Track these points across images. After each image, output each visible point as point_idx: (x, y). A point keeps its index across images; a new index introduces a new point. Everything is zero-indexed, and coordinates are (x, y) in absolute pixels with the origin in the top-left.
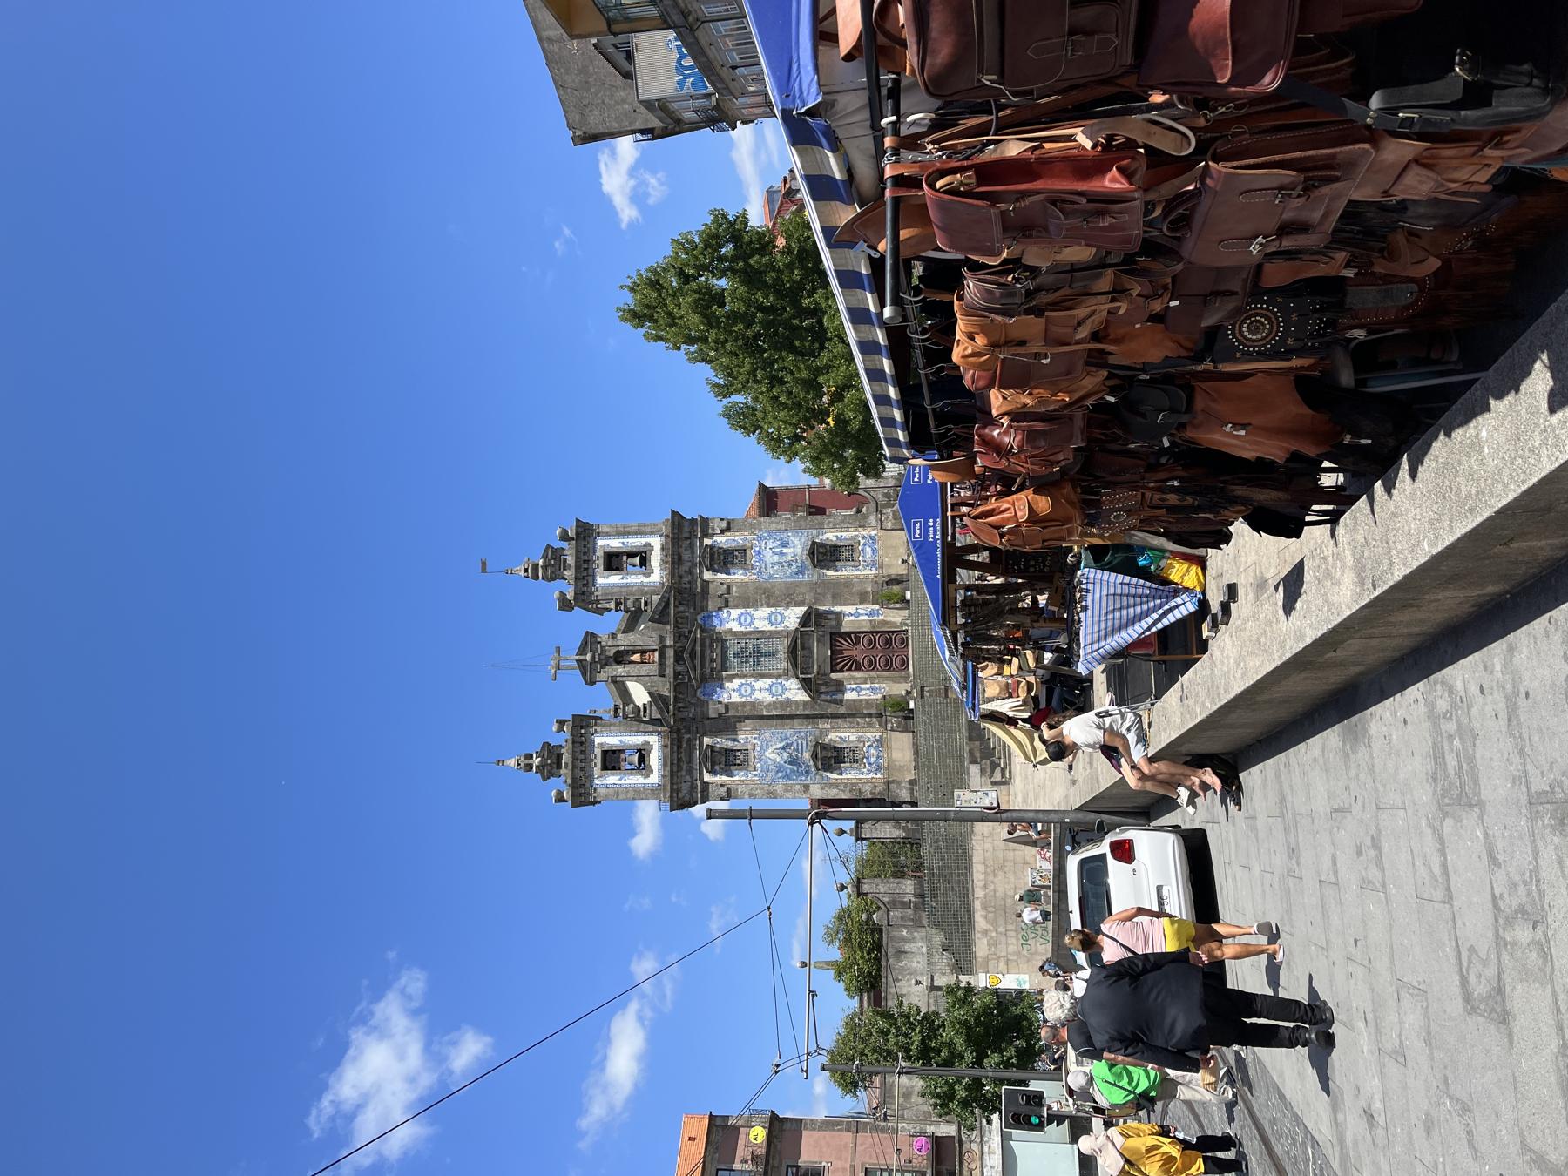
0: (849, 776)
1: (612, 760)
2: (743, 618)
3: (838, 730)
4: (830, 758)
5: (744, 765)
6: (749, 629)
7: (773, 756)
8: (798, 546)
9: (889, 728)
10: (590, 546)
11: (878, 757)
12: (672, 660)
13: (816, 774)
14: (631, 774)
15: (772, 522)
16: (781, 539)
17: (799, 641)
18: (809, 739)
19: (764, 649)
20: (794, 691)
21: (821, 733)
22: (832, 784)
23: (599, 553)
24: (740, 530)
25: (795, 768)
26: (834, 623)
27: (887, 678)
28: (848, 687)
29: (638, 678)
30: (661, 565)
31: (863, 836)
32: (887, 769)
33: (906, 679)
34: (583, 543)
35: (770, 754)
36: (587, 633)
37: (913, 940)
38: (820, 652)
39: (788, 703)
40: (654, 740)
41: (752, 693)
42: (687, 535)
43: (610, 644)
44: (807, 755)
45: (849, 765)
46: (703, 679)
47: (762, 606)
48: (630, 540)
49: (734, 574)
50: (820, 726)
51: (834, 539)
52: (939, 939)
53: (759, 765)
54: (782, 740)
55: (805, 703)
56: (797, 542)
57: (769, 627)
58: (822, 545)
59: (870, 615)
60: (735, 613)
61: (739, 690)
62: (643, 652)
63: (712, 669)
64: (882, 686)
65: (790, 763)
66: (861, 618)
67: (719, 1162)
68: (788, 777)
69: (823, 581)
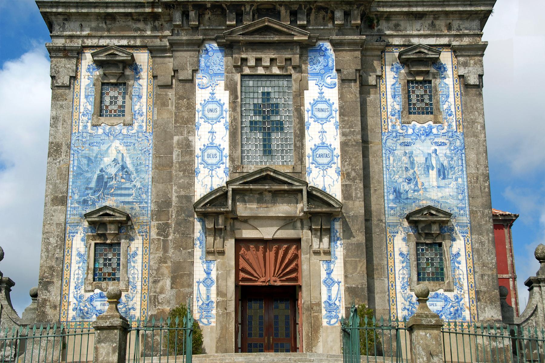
0: (74, 266)
4: (103, 236)
6: (307, 116)
15: (477, 155)
16: (452, 168)
17: (286, 187)
18: (136, 206)
21: (142, 225)
24: (464, 105)
25: (93, 185)
27: (224, 329)
28: (213, 267)
41: (207, 120)
44: (110, 202)
45: (92, 266)
47: (343, 134)
49: (394, 97)
50: (154, 223)
51: (454, 250)
55: (189, 198)
56: (447, 192)
57: (309, 143)
58: (442, 224)
59: (330, 305)
60: (333, 95)
61: (213, 99)
63: (244, 60)
65: (100, 178)
68: (79, 174)
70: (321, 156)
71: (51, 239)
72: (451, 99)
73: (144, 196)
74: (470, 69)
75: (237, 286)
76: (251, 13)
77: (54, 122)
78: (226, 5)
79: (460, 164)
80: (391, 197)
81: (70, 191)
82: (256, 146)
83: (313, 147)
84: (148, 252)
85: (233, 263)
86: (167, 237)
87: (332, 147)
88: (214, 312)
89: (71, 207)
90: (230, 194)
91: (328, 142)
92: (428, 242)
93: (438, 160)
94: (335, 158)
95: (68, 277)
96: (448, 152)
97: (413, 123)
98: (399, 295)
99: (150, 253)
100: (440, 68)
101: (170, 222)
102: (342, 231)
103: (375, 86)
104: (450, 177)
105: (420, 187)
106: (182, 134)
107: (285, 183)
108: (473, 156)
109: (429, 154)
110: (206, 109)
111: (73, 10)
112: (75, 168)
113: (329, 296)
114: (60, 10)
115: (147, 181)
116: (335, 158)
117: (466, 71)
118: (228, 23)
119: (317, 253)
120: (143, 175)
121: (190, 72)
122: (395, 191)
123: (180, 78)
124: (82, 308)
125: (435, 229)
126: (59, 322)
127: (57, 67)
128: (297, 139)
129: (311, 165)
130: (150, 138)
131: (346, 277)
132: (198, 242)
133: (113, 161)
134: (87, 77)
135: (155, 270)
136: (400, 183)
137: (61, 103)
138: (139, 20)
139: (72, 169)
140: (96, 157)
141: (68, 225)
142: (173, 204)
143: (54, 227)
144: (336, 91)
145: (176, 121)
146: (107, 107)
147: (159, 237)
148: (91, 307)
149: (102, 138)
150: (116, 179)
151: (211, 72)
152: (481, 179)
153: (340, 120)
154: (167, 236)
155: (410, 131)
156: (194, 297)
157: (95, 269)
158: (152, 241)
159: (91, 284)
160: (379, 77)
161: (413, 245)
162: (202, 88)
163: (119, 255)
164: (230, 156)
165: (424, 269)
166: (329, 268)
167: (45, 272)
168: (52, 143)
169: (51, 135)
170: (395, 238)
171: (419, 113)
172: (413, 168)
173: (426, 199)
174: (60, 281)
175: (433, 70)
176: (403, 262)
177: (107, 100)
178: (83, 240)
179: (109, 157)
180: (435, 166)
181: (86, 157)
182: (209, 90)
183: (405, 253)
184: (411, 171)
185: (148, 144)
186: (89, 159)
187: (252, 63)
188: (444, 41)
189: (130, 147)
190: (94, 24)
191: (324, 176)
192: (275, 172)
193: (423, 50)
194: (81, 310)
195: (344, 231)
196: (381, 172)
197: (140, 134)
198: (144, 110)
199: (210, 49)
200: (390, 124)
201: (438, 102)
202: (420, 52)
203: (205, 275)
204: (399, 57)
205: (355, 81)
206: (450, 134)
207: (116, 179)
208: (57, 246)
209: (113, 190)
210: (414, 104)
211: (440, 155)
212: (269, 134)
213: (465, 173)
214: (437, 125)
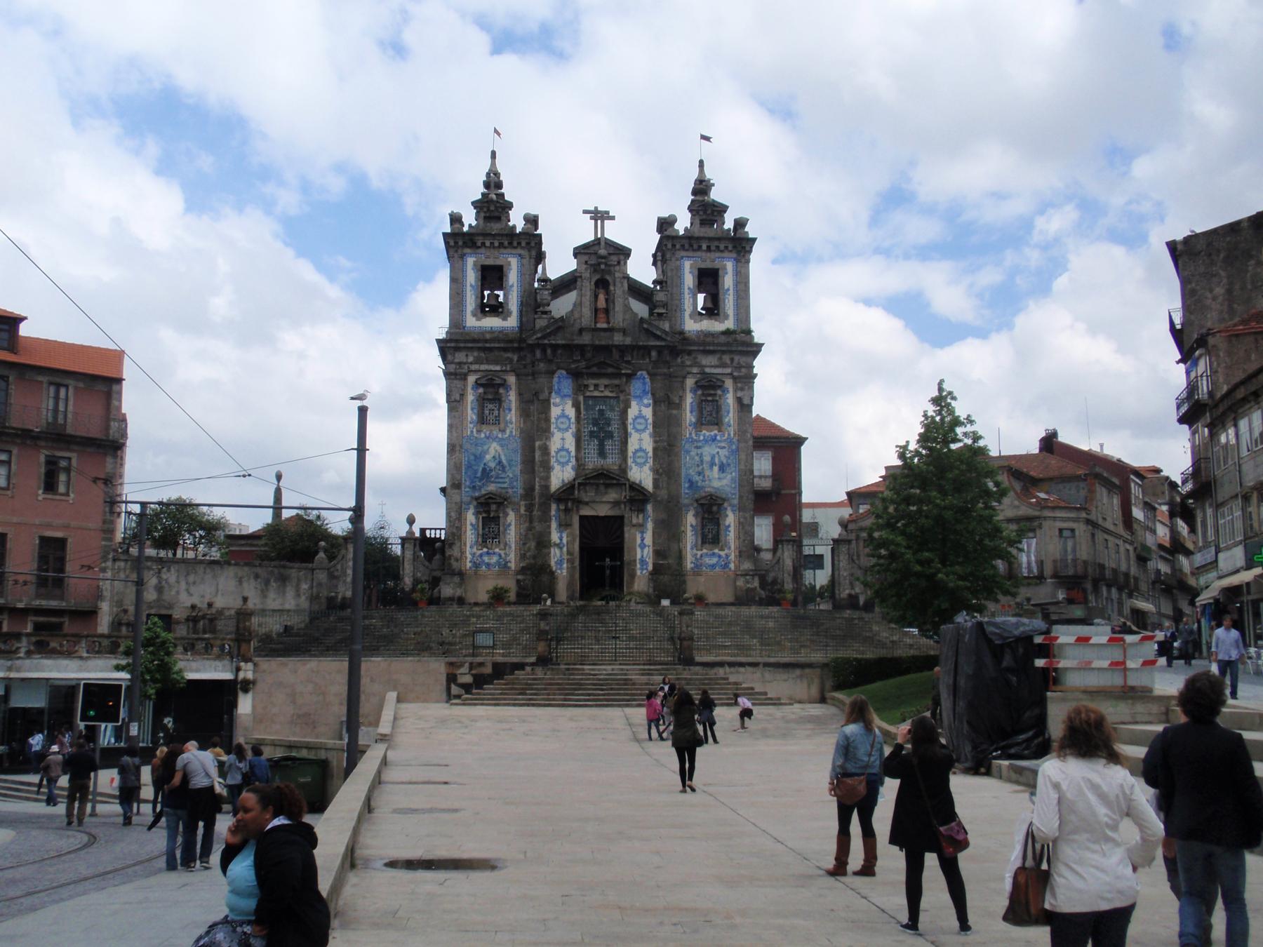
1: (492, 276)
2: (642, 421)
3: (518, 525)
4: (488, 512)
5: (482, 420)
7: (492, 452)
8: (720, 482)
9: (520, 577)
10: (726, 254)
11: (488, 565)
12: (597, 343)
13: (472, 497)
14: (477, 297)
15: (746, 455)
16: (729, 465)
18: (510, 490)
19: (608, 444)
20: (561, 475)
23: (717, 264)
24: (740, 418)
25: (479, 475)
26: (635, 521)
27: (571, 575)
29: (578, 305)
30: (701, 331)
31: (406, 546)
32: (476, 573)
33: (571, 598)
34: (730, 248)
35: (494, 449)
36: (630, 250)
37: (298, 595)
38: (601, 505)
39: (548, 468)
40: (512, 322)
41: (560, 429)
43: (617, 275)
44: (492, 488)
45: (481, 532)
46: (576, 375)
47: (655, 442)
49: (691, 412)
50: (523, 503)
51: (727, 524)
52: (296, 621)
53: (483, 435)
54: (510, 461)
55: (547, 487)
56: (725, 482)
58: (720, 505)
59: (643, 561)
60: (648, 412)
61: (563, 415)
62: (607, 311)
63: (586, 386)
64: (565, 572)
65: (484, 470)
67: (76, 388)
68: (469, 466)
70: (639, 457)
72: (731, 415)
74: (745, 392)
75: (581, 549)
80: (687, 485)
85: (578, 532)
88: (565, 565)
90: (576, 486)
96: (727, 453)
97: (704, 432)
98: (688, 554)
99: (521, 524)
100: (723, 391)
103: (679, 404)
106: (541, 440)
107: (614, 479)
108: (743, 456)
111: (462, 345)
113: (642, 556)
114: (453, 345)
118: (575, 358)
119: (634, 526)
120: (514, 468)
121: (547, 394)
123: (541, 398)
125: (715, 508)
126: (461, 570)
131: (654, 542)
138: (509, 351)
140: (480, 454)
142: (537, 491)
143: (453, 505)
144: (651, 408)
145: (538, 431)
151: (562, 394)
152: (748, 473)
154: (532, 511)
155: (702, 438)
157: (483, 535)
158: (521, 516)
160: (681, 397)
161: (699, 519)
163: (499, 525)
165: (707, 535)
172: (702, 464)
173: (710, 487)
175: (719, 392)
177: (487, 412)
182: (561, 407)
184: (701, 467)
185: (516, 444)
186: (475, 456)
187: (592, 388)
188: (728, 371)
190: (476, 354)
191: (641, 472)
192: (607, 471)
198: (514, 420)
202: (711, 381)
204: (696, 383)
205: (664, 402)
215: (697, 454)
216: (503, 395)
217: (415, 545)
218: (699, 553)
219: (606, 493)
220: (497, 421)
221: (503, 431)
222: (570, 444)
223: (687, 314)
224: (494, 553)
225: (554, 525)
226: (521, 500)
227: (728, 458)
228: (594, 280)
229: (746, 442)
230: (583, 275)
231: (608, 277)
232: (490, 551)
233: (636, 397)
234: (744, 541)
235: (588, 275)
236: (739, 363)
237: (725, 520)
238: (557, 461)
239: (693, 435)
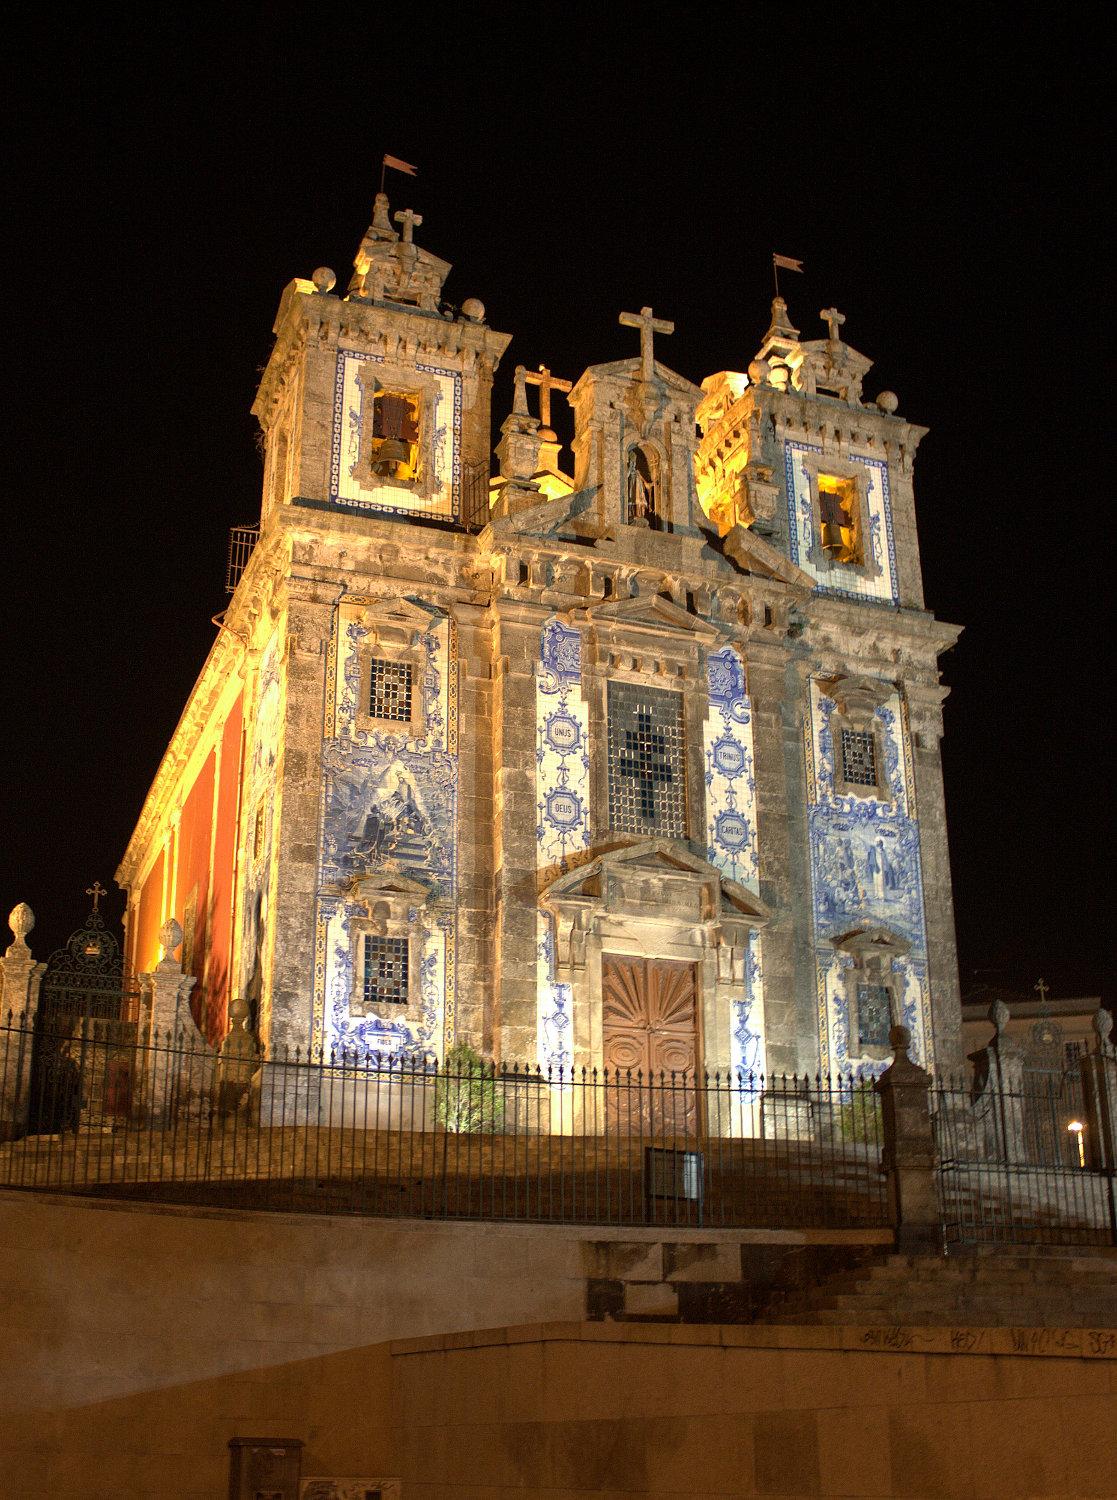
0: (332, 971)
3: (453, 958)
6: (708, 762)
10: (869, 451)
15: (937, 859)
16: (903, 873)
18: (434, 878)
19: (662, 790)
22: (312, 923)
25: (360, 832)
26: (725, 973)
41: (555, 747)
42: (904, 658)
43: (675, 440)
45: (361, 973)
47: (761, 800)
48: (883, 534)
49: (823, 750)
51: (908, 1002)
53: (371, 742)
54: (434, 808)
56: (899, 908)
60: (744, 734)
61: (562, 715)
63: (614, 661)
65: (372, 822)
66: (735, 1043)
68: (335, 812)
69: (810, 960)
70: (729, 830)
71: (292, 919)
73: (446, 862)
74: (926, 724)
76: (628, 583)
77: (294, 714)
78: (592, 563)
79: (914, 868)
80: (822, 908)
81: (322, 839)
82: (631, 800)
83: (718, 815)
84: (453, 959)
86: (485, 937)
87: (746, 818)
89: (324, 868)
91: (739, 810)
92: (875, 984)
93: (884, 858)
94: (750, 837)
95: (322, 989)
96: (898, 848)
97: (851, 795)
99: (457, 962)
101: (488, 911)
102: (760, 955)
104: (901, 886)
105: (861, 897)
106: (515, 767)
108: (930, 858)
109: (873, 848)
110: (553, 728)
112: (329, 800)
113: (744, 1058)
115: (449, 837)
116: (750, 837)
117: (921, 728)
120: (443, 827)
122: (826, 899)
124: (347, 1044)
127: (299, 620)
128: (694, 798)
129: (715, 843)
130: (453, 764)
131: (767, 1028)
132: (543, 951)
133: (394, 796)
134: (348, 645)
135: (467, 991)
136: (835, 888)
137: (304, 682)
139: (323, 801)
140: (364, 785)
141: (319, 898)
142: (504, 882)
143: (295, 900)
145: (505, 743)
146: (380, 701)
147: (472, 936)
148: (362, 1044)
149: (373, 753)
150: (398, 828)
153: (755, 774)
155: (847, 808)
156: (540, 1039)
157: (367, 981)
159: (361, 1004)
161: (852, 987)
162: (547, 693)
163: (406, 959)
164: (591, 812)
165: (867, 1025)
166: (742, 1013)
167: (282, 977)
168: (290, 751)
169: (287, 736)
170: (829, 973)
171: (857, 781)
172: (851, 867)
173: (869, 916)
174: (309, 994)
176: (839, 1013)
178: (344, 926)
179: (386, 787)
180: (880, 866)
181: (347, 783)
182: (557, 697)
183: (842, 997)
184: (849, 871)
185: (453, 773)
186: (353, 788)
189: (421, 776)
193: (868, 683)
194: (345, 1047)
195: (764, 956)
196: (805, 866)
197: (438, 756)
198: (444, 715)
199: (559, 630)
200: (819, 792)
201: (883, 769)
203: (556, 1009)
206: (901, 819)
207: (398, 828)
208: (301, 933)
209: (394, 846)
210: (850, 767)
211: (888, 851)
212: (650, 784)
213: (920, 883)
214: (884, 803)
215: (840, 843)
216: (421, 657)
217: (180, 998)
218: (855, 1063)
219: (666, 902)
220: (405, 713)
221: (421, 738)
222: (580, 782)
223: (803, 549)
224: (394, 1029)
225: (543, 967)
226: (459, 902)
227: (901, 857)
228: (627, 442)
229: (934, 828)
230: (606, 426)
231: (656, 444)
232: (385, 1022)
233: (714, 696)
234: (944, 1041)
235: (617, 429)
236: (909, 663)
237: (904, 993)
238: (550, 817)
239: (830, 800)
